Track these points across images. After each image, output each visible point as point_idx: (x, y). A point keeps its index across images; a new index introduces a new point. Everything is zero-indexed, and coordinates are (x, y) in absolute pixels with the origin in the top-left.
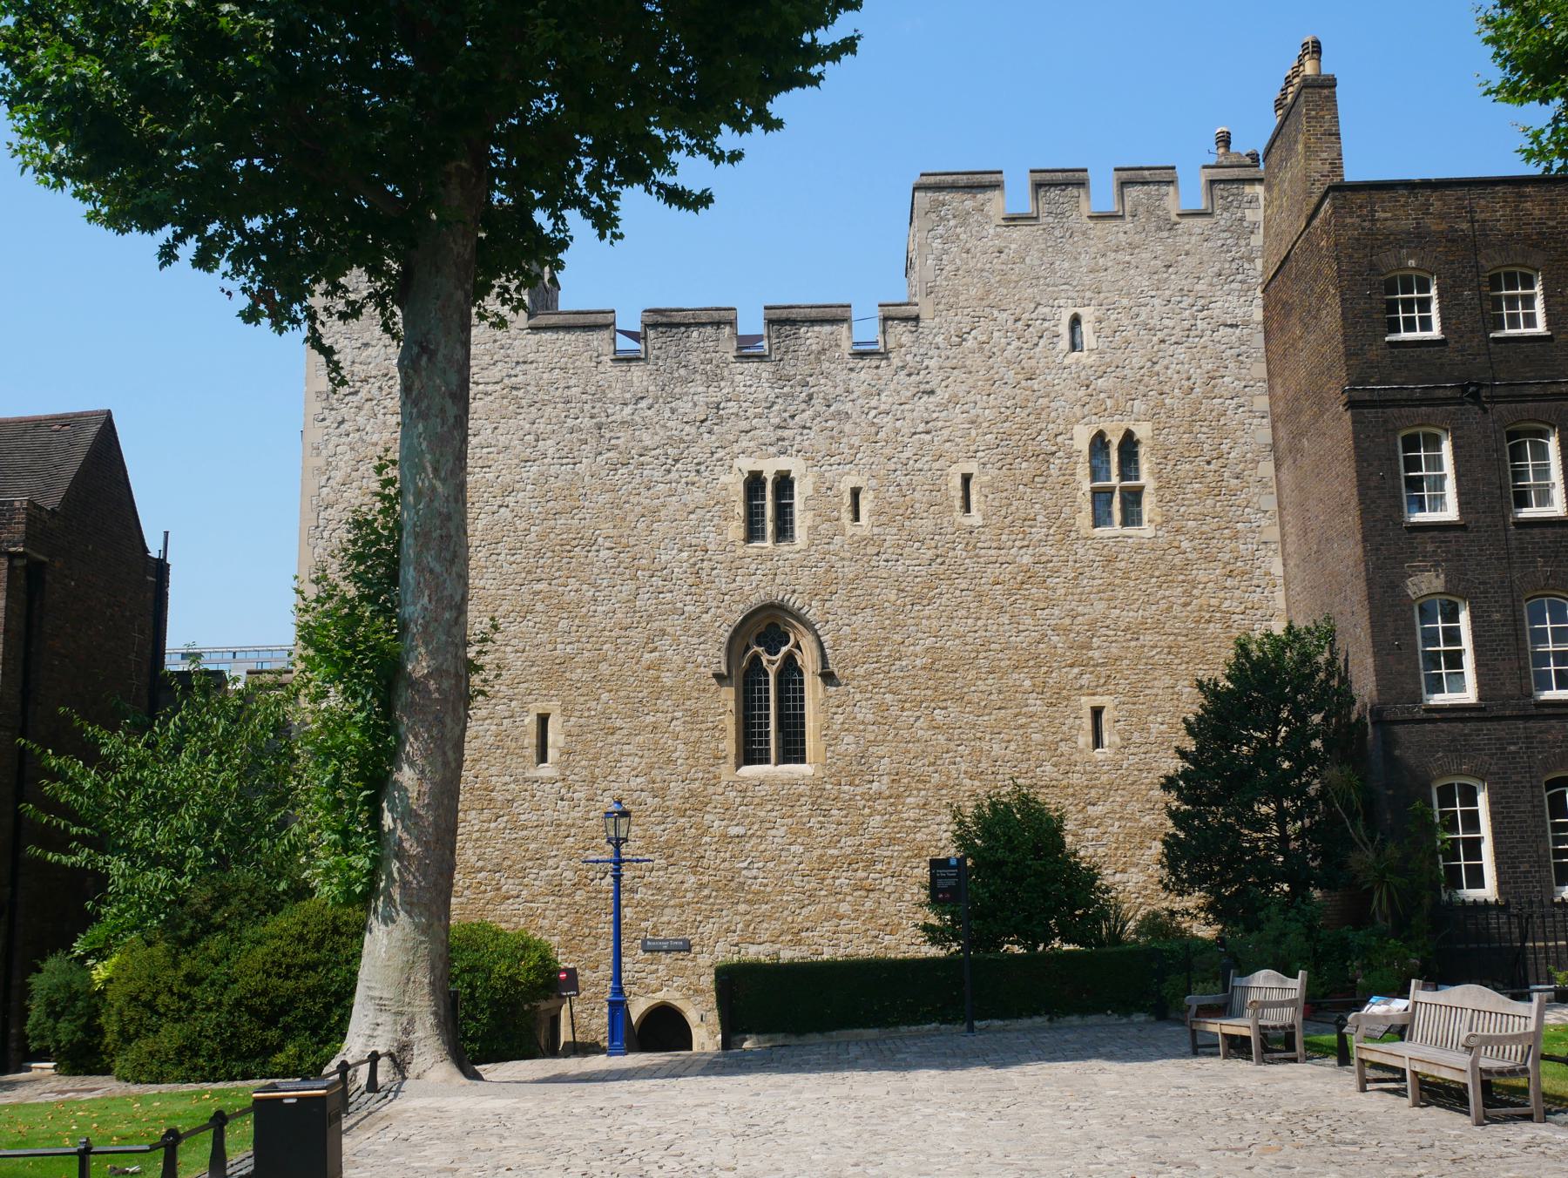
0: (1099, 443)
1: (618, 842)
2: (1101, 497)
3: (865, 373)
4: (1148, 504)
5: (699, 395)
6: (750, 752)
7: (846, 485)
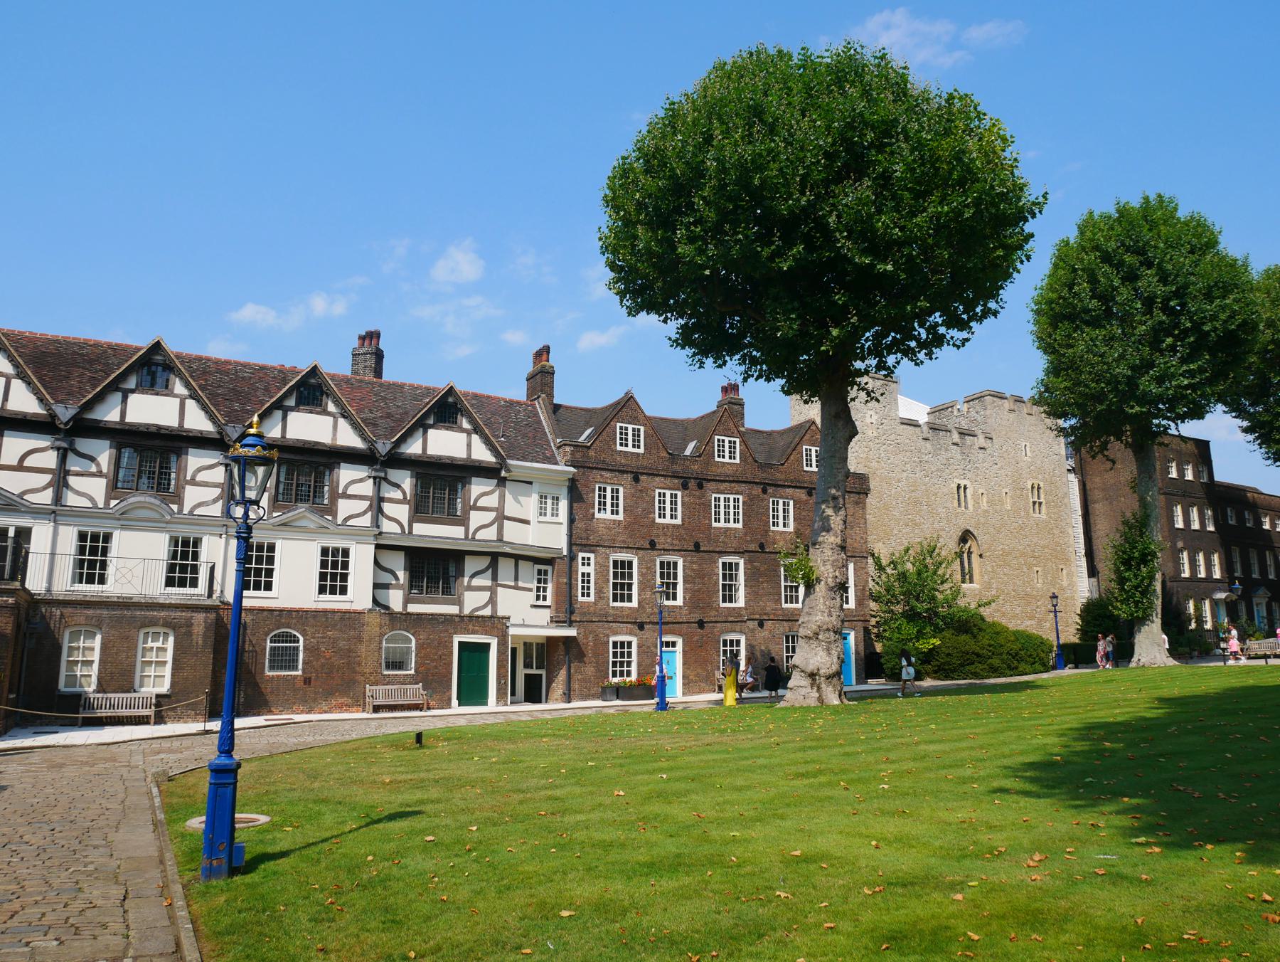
0: (1033, 487)
1: (1055, 606)
2: (1034, 503)
3: (981, 455)
4: (1043, 506)
5: (943, 456)
6: (963, 582)
7: (981, 491)
